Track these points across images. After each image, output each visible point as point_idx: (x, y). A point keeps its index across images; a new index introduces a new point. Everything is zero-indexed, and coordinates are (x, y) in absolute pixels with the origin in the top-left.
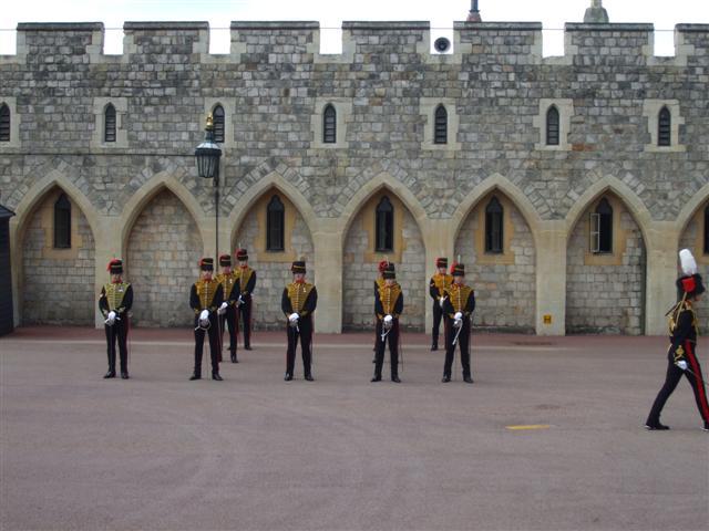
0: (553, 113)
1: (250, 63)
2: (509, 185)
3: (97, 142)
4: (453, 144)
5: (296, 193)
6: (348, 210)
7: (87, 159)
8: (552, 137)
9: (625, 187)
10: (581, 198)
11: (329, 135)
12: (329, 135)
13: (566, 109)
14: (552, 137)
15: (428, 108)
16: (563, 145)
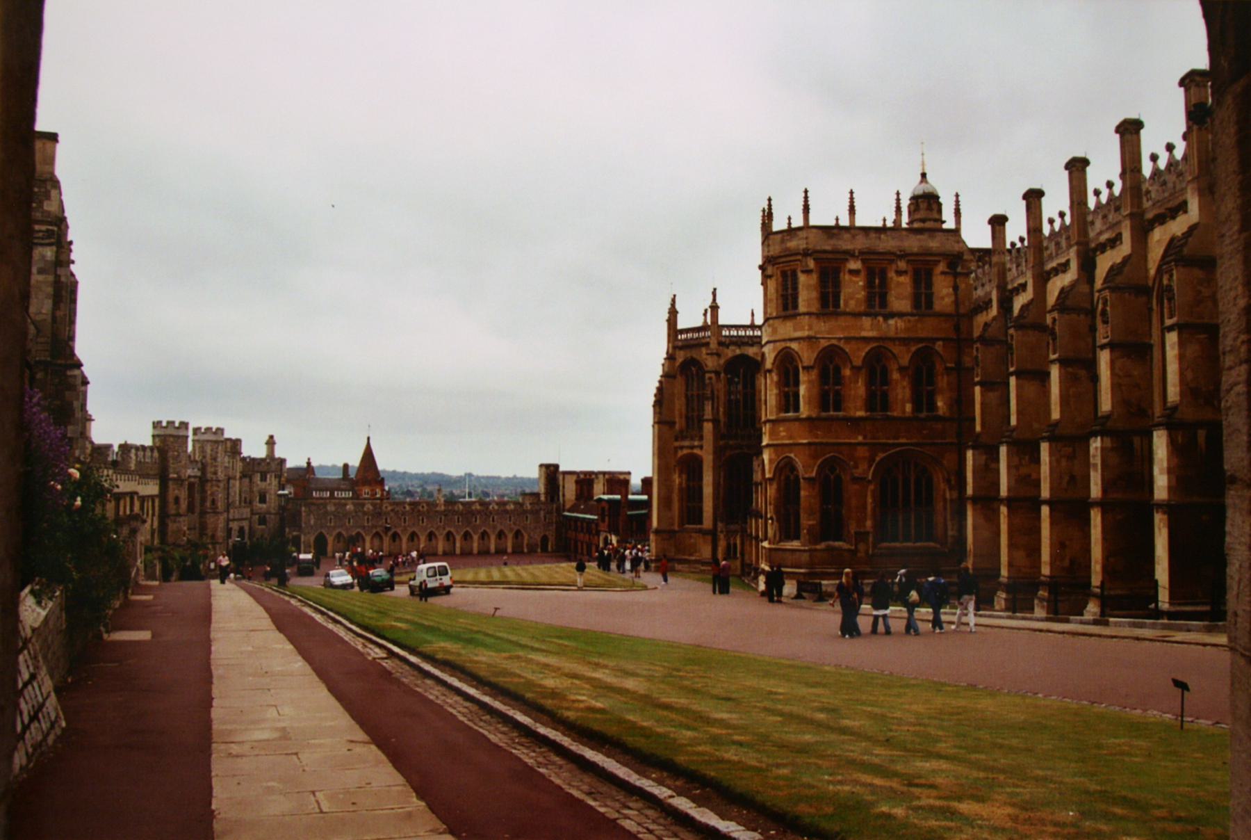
0: (441, 519)
1: (392, 510)
2: (434, 530)
3: (366, 524)
4: (425, 524)
5: (399, 532)
6: (408, 535)
7: (364, 527)
8: (441, 522)
9: (452, 530)
10: (445, 532)
11: (405, 522)
12: (405, 522)
13: (443, 518)
14: (441, 522)
15: (421, 518)
16: (442, 524)
